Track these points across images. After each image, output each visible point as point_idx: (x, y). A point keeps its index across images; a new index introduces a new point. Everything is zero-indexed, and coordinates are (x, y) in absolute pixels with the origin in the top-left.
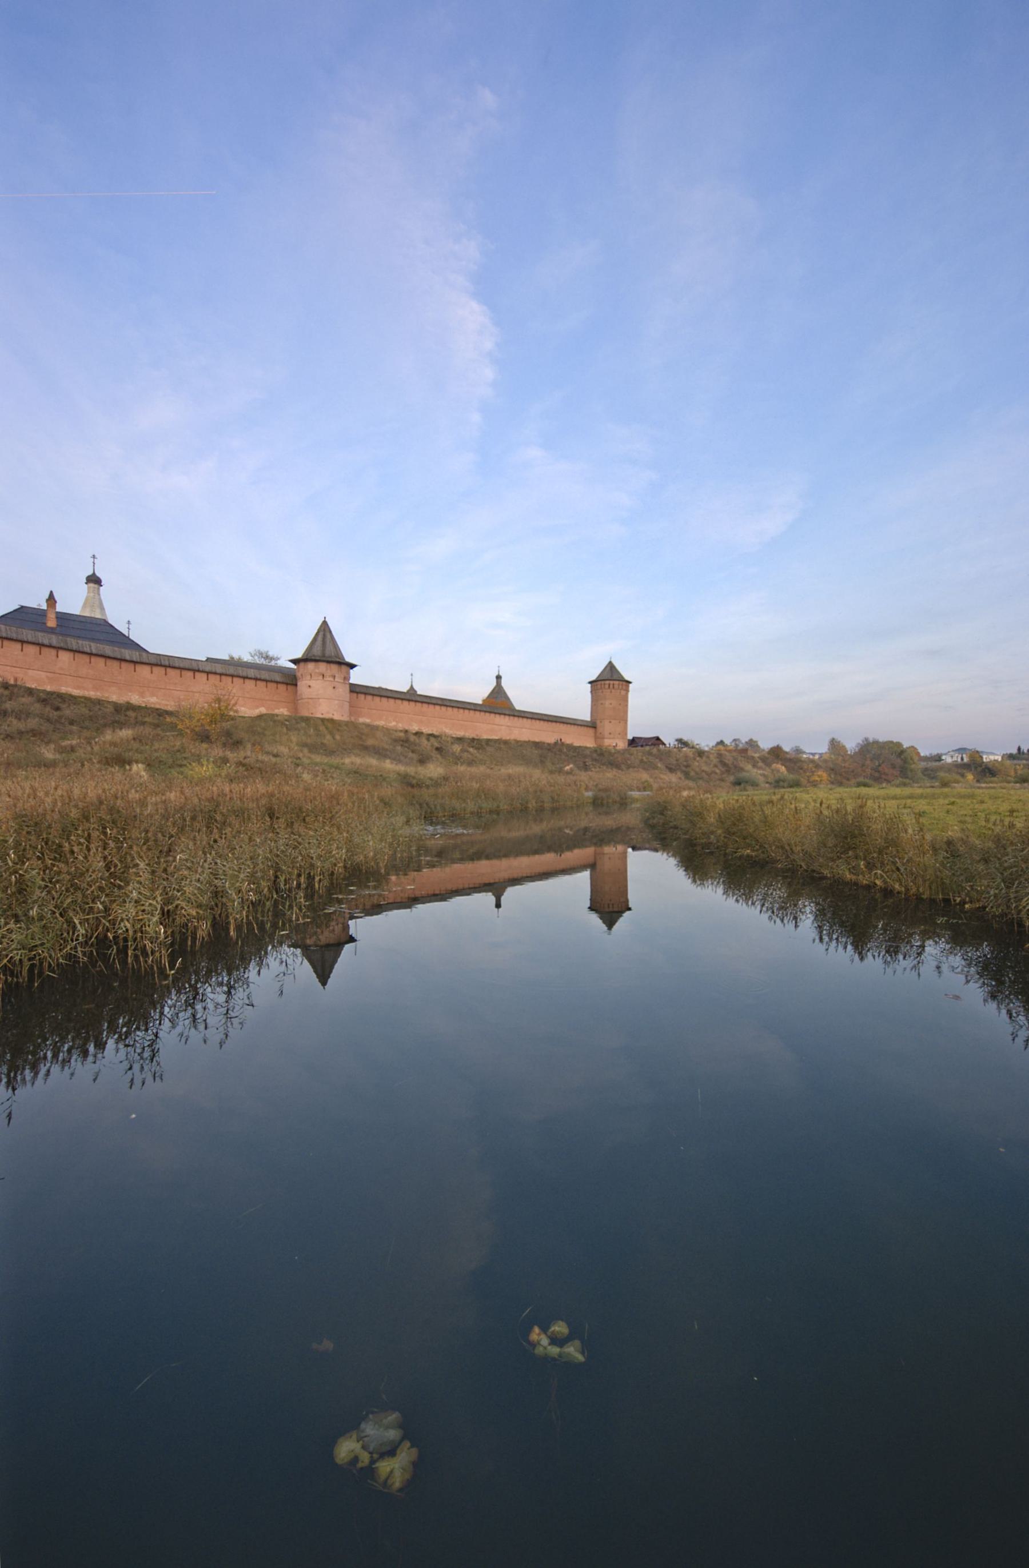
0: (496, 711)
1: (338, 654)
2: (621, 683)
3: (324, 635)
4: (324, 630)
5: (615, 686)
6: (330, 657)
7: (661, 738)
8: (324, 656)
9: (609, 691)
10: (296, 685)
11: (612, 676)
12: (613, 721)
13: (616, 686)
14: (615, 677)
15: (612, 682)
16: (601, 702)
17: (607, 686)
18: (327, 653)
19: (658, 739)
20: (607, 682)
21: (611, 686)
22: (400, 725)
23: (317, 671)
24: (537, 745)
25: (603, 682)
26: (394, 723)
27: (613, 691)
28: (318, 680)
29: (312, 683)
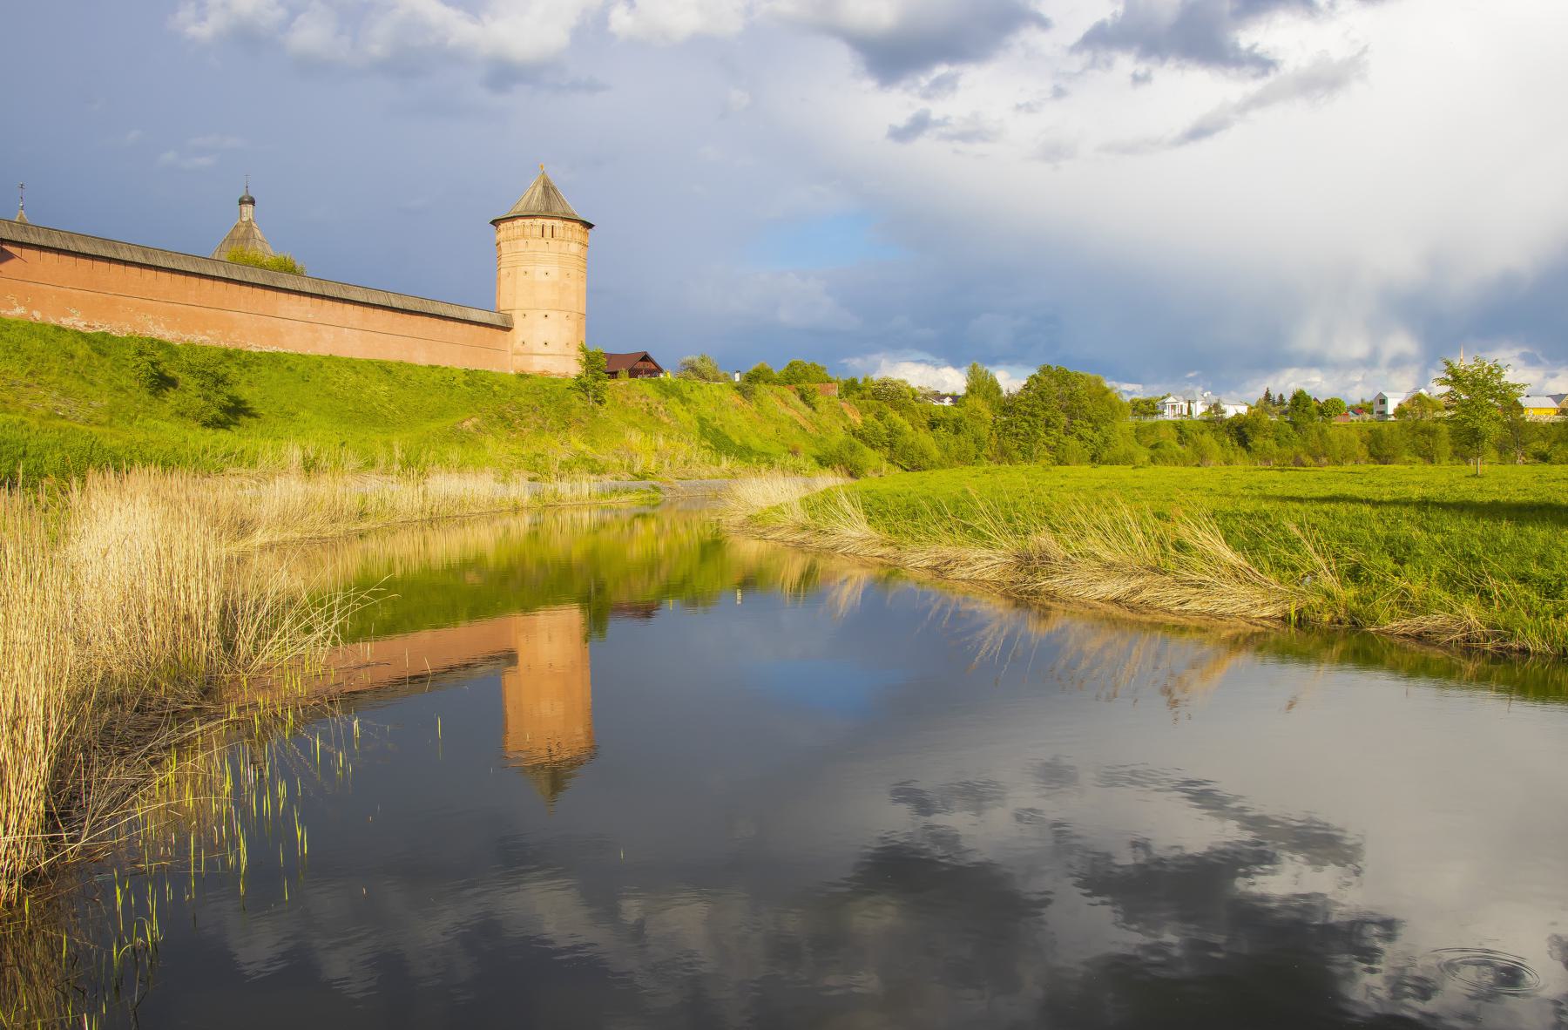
2: (570, 224)
7: (652, 355)
9: (543, 241)
11: (547, 210)
12: (552, 315)
14: (558, 210)
15: (548, 222)
16: (524, 268)
17: (538, 231)
19: (646, 358)
20: (540, 221)
21: (548, 232)
24: (385, 370)
25: (528, 221)
26: (19, 311)
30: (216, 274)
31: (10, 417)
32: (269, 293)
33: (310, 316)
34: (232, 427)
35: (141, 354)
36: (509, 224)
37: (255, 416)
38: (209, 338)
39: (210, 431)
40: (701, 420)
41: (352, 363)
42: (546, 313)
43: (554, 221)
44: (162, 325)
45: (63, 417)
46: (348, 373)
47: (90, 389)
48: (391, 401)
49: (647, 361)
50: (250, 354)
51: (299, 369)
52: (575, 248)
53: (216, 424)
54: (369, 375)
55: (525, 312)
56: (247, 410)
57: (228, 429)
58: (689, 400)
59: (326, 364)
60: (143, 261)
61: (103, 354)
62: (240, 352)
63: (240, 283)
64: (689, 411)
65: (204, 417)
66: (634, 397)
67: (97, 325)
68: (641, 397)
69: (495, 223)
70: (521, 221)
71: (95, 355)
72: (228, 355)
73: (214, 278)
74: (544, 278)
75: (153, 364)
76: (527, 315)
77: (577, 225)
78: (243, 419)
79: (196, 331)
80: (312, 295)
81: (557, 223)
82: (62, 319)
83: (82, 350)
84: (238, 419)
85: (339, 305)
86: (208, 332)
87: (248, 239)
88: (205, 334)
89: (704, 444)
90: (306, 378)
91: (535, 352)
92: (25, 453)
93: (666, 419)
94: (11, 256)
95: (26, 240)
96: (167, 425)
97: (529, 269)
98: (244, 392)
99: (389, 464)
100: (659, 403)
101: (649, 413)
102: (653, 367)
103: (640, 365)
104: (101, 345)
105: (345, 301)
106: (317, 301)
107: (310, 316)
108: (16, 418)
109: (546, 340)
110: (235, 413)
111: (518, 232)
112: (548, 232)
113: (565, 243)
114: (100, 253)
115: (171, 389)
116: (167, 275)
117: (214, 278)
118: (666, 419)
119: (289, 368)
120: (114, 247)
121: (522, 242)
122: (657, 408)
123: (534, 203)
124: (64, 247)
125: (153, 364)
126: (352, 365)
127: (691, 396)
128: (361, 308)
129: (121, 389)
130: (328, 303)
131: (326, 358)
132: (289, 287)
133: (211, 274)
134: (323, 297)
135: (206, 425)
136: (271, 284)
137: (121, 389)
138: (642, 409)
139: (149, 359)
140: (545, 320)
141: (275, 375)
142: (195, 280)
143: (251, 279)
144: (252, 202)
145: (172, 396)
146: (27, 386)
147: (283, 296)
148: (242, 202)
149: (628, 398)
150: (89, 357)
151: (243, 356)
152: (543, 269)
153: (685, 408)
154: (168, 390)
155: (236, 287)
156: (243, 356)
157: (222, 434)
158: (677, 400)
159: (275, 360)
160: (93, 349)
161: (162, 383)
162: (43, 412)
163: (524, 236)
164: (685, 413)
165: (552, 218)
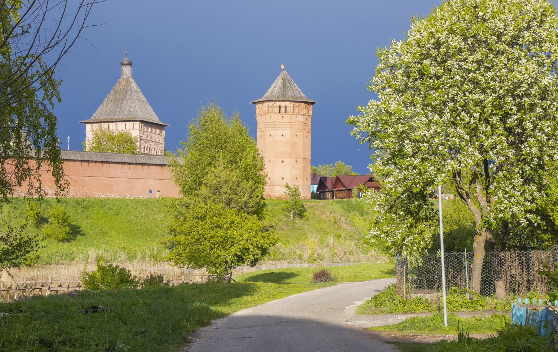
0: (110, 160)
2: (297, 104)
5: (288, 109)
9: (280, 116)
11: (284, 96)
12: (287, 161)
13: (289, 110)
15: (283, 104)
20: (278, 104)
21: (283, 110)
25: (271, 104)
27: (285, 116)
30: (75, 159)
32: (105, 165)
33: (129, 174)
34: (72, 241)
36: (260, 105)
37: (84, 235)
39: (61, 244)
41: (146, 203)
42: (283, 159)
48: (162, 223)
50: (89, 201)
51: (115, 208)
52: (301, 118)
53: (63, 240)
54: (154, 209)
55: (270, 159)
57: (70, 242)
58: (367, 213)
59: (130, 204)
62: (84, 201)
63: (89, 161)
64: (365, 220)
65: (58, 237)
66: (326, 213)
68: (331, 212)
71: (12, 210)
73: (74, 161)
74: (281, 138)
75: (37, 214)
76: (271, 161)
77: (302, 104)
78: (79, 237)
80: (129, 164)
81: (289, 104)
84: (75, 237)
85: (146, 167)
87: (127, 91)
90: (117, 213)
91: (276, 184)
93: (345, 226)
97: (273, 133)
98: (84, 224)
99: (143, 258)
100: (342, 216)
101: (335, 222)
105: (149, 165)
106: (132, 166)
107: (129, 174)
109: (283, 176)
111: (266, 110)
112: (283, 110)
113: (294, 116)
115: (45, 223)
117: (74, 161)
118: (345, 226)
119: (110, 208)
121: (268, 116)
125: (37, 214)
126: (146, 203)
128: (160, 167)
131: (132, 201)
132: (116, 161)
134: (136, 164)
135: (59, 241)
138: (330, 220)
139: (35, 212)
140: (282, 164)
141: (101, 212)
143: (95, 159)
144: (130, 64)
147: (112, 166)
148: (122, 65)
149: (323, 213)
150: (9, 212)
151: (85, 203)
152: (281, 133)
153: (362, 218)
154: (43, 225)
155: (86, 164)
156: (85, 203)
157: (66, 245)
158: (357, 213)
159: (103, 203)
164: (362, 222)
165: (285, 101)
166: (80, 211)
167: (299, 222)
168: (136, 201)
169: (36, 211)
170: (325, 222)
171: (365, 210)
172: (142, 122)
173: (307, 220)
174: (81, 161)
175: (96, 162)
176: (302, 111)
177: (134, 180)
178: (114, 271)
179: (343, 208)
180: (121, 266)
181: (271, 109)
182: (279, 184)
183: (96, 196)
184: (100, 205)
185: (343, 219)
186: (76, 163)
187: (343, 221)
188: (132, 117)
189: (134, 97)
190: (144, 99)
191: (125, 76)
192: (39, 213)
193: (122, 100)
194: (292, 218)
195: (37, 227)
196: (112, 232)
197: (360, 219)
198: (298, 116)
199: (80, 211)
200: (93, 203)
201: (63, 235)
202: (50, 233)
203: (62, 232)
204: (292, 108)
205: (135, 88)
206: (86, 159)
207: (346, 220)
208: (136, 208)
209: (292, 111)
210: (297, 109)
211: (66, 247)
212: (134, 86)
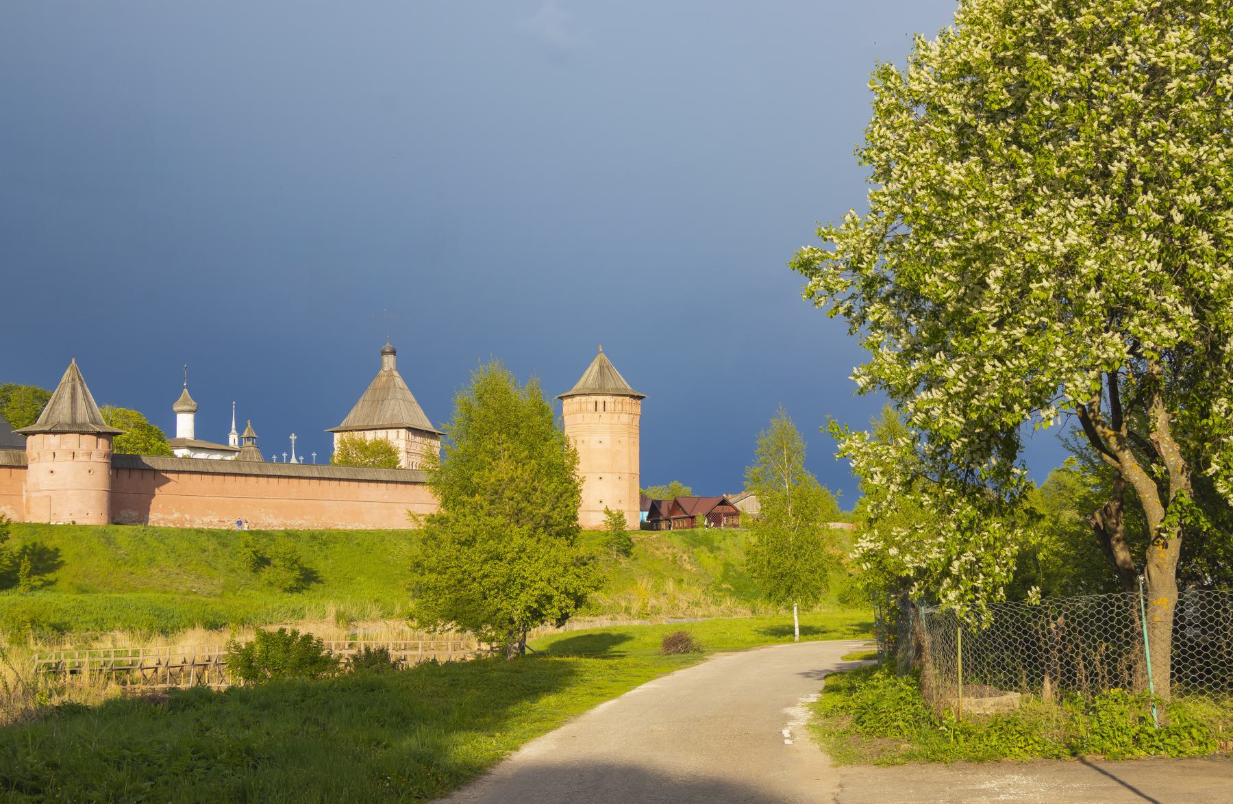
0: (360, 478)
1: (95, 419)
2: (620, 398)
3: (74, 388)
4: (73, 380)
6: (83, 424)
8: (74, 422)
9: (597, 415)
10: (26, 467)
12: (607, 477)
15: (600, 399)
18: (79, 420)
20: (593, 398)
21: (600, 406)
22: (187, 516)
23: (64, 447)
25: (583, 398)
26: (176, 515)
27: (604, 415)
28: (66, 460)
29: (54, 466)
31: (167, 596)
34: (305, 591)
35: (247, 546)
36: (569, 400)
37: (321, 582)
38: (300, 523)
39: (286, 595)
40: (727, 565)
42: (601, 475)
43: (606, 397)
44: (272, 516)
45: (195, 593)
46: (404, 545)
47: (215, 573)
49: (726, 505)
52: (625, 418)
53: (291, 590)
56: (317, 577)
58: (719, 548)
59: (388, 538)
60: (258, 473)
61: (225, 545)
62: (322, 533)
64: (716, 558)
66: (662, 548)
67: (226, 519)
68: (668, 548)
69: (561, 398)
70: (578, 398)
71: (219, 548)
72: (314, 536)
75: (254, 552)
78: (313, 585)
79: (296, 518)
80: (387, 482)
81: (609, 399)
82: (203, 518)
83: (211, 545)
84: (309, 585)
86: (305, 517)
87: (389, 388)
88: (303, 519)
89: (724, 586)
92: (173, 616)
93: (688, 567)
94: (168, 480)
95: (181, 469)
96: (257, 594)
98: (321, 566)
100: (684, 552)
101: (674, 562)
102: (732, 510)
103: (720, 509)
104: (222, 538)
108: (169, 597)
110: (307, 579)
111: (576, 407)
112: (600, 406)
113: (616, 416)
114: (229, 471)
115: (266, 566)
116: (276, 480)
117: (310, 478)
118: (688, 567)
119: (358, 544)
120: (239, 465)
121: (580, 416)
122: (682, 557)
123: (590, 381)
124: (205, 471)
127: (722, 545)
129: (233, 571)
130: (400, 486)
133: (308, 475)
135: (285, 590)
136: (354, 478)
137: (233, 571)
138: (668, 558)
140: (600, 482)
142: (295, 481)
143: (338, 476)
144: (394, 352)
145: (267, 574)
146: (177, 574)
148: (384, 353)
149: (657, 549)
150: (215, 550)
151: (324, 538)
153: (712, 556)
156: (324, 538)
158: (705, 549)
159: (348, 536)
160: (219, 544)
161: (261, 562)
162: (185, 590)
163: (581, 411)
165: (603, 394)
166: (316, 548)
167: (624, 562)
168: (395, 534)
169: (254, 549)
170: (661, 560)
171: (716, 544)
172: (409, 429)
173: (635, 559)
174: (320, 479)
175: (340, 480)
176: (627, 408)
177: (394, 505)
178: (288, 642)
179: (685, 542)
180: (303, 632)
181: (584, 406)
182: (597, 509)
183: (341, 528)
184: (344, 540)
185: (685, 557)
186: (312, 481)
187: (685, 560)
188: (395, 422)
189: (399, 396)
190: (413, 399)
191: (386, 369)
192: (258, 551)
193: (383, 400)
194: (615, 557)
195: (255, 571)
196: (361, 579)
197: (709, 557)
198: (622, 416)
199: (316, 548)
200: (334, 538)
201: (292, 583)
202: (272, 579)
203: (291, 577)
204: (613, 404)
205: (401, 384)
206: (327, 476)
207: (689, 558)
208: (395, 544)
209: (613, 408)
210: (620, 406)
211: (296, 599)
212: (399, 381)
